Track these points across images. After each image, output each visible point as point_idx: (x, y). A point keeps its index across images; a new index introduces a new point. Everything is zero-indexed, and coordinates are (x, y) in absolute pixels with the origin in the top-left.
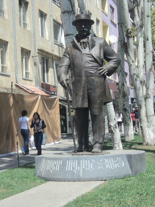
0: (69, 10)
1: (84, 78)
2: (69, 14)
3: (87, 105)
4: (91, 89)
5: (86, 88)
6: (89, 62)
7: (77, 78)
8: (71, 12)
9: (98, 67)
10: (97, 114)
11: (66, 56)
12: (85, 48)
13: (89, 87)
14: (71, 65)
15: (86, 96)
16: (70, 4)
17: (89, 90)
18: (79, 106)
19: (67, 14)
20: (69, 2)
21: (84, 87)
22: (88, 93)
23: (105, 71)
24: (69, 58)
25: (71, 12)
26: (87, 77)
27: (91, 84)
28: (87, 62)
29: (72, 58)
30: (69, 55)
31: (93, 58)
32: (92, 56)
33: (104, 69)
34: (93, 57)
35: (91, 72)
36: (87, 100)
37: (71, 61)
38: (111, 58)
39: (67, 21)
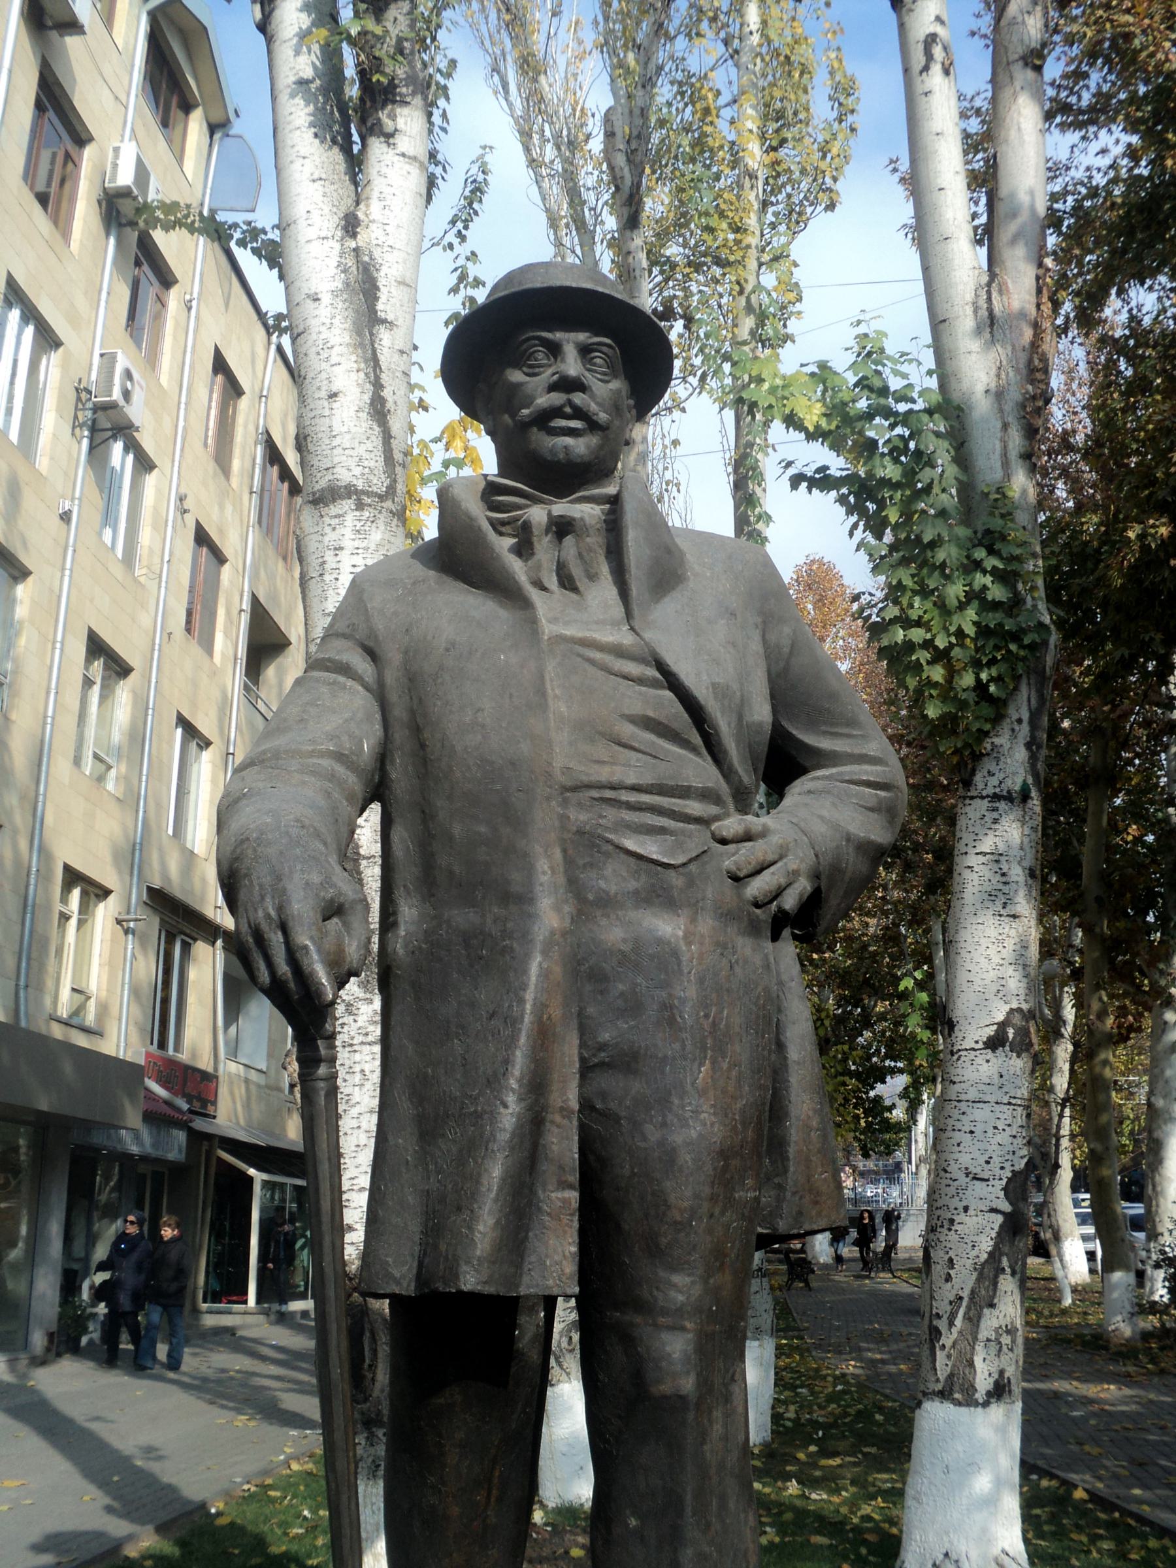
0: (369, 481)
1: (549, 914)
2: (360, 506)
3: (570, 1268)
4: (626, 1061)
5: (569, 1052)
6: (628, 730)
7: (462, 917)
8: (382, 498)
9: (713, 810)
10: (688, 1384)
11: (345, 670)
12: (567, 582)
13: (605, 1036)
14: (400, 773)
15: (563, 1143)
16: (377, 441)
17: (602, 1065)
18: (470, 1281)
19: (348, 504)
20: (375, 427)
21: (544, 1035)
22: (586, 1105)
23: (792, 863)
24: (380, 695)
25: (382, 498)
26: (587, 904)
27: (632, 1007)
28: (603, 734)
29: (413, 681)
30: (372, 654)
31: (668, 694)
32: (661, 666)
33: (775, 839)
34: (672, 682)
35: (651, 848)
36: (573, 1196)
37: (399, 712)
38: (825, 744)
39: (344, 556)
